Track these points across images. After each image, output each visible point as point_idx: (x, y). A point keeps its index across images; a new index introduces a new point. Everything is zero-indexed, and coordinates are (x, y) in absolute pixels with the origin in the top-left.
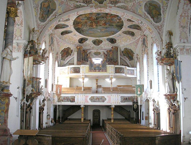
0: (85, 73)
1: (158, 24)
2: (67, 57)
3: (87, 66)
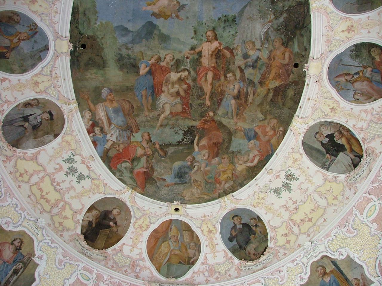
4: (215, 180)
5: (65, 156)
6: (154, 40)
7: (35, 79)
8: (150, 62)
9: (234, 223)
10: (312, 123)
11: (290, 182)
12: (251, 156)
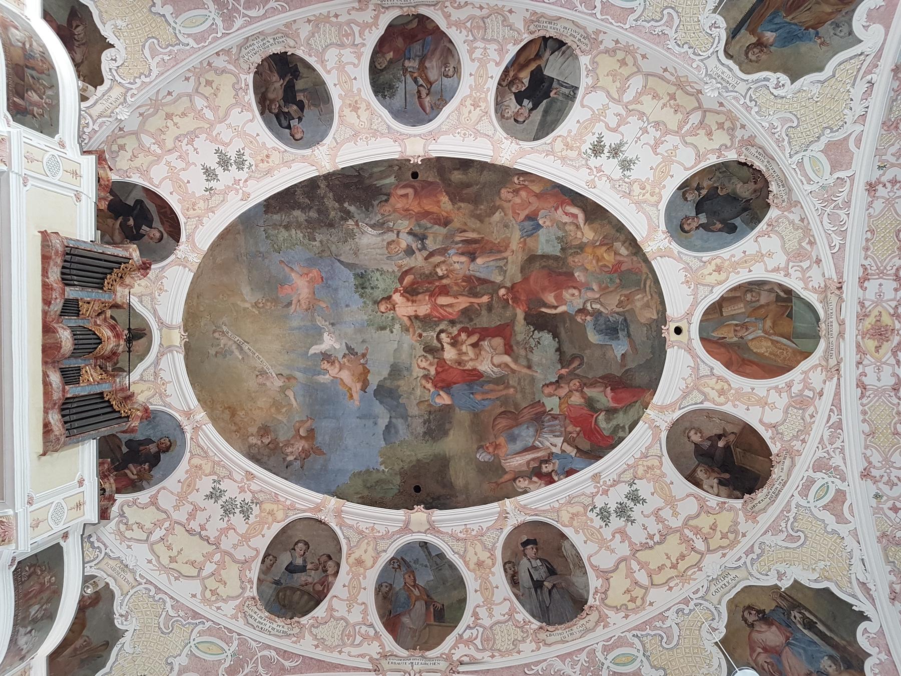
4: (616, 271)
5: (598, 522)
6: (399, 386)
7: (472, 566)
8: (432, 390)
9: (697, 228)
10: (501, 133)
11: (607, 147)
12: (566, 219)
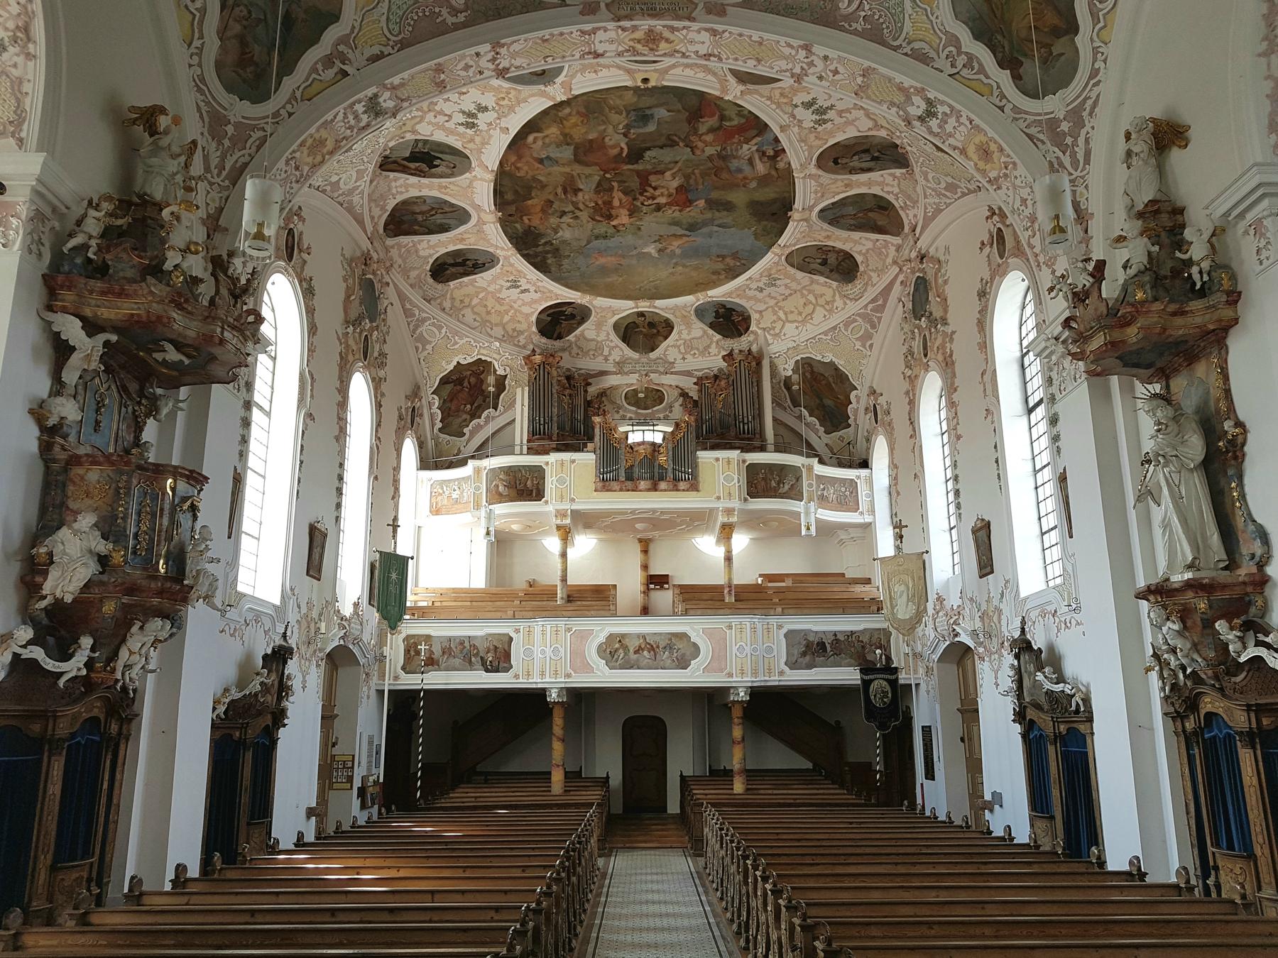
0: (573, 500)
1: (1054, 105)
2: (475, 415)
3: (586, 460)
12: (540, 143)
